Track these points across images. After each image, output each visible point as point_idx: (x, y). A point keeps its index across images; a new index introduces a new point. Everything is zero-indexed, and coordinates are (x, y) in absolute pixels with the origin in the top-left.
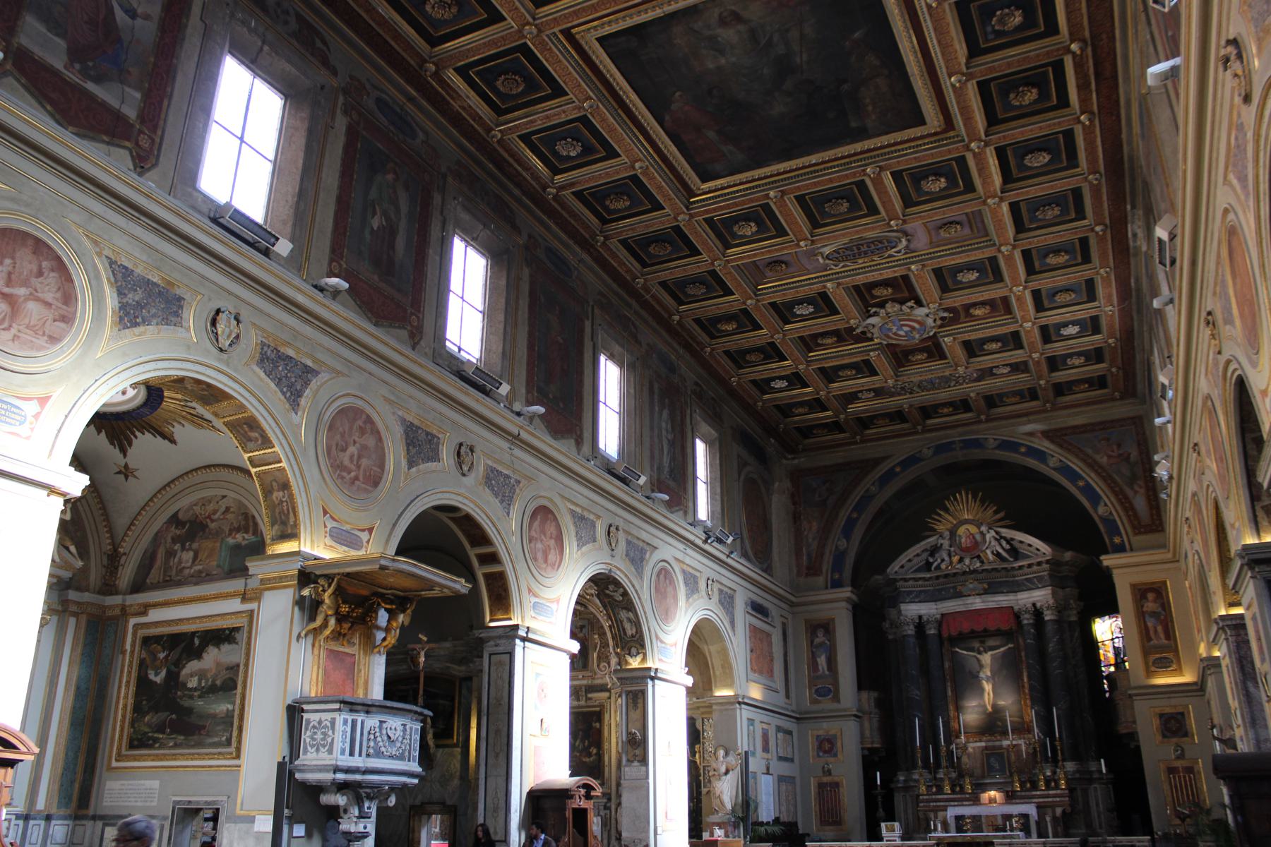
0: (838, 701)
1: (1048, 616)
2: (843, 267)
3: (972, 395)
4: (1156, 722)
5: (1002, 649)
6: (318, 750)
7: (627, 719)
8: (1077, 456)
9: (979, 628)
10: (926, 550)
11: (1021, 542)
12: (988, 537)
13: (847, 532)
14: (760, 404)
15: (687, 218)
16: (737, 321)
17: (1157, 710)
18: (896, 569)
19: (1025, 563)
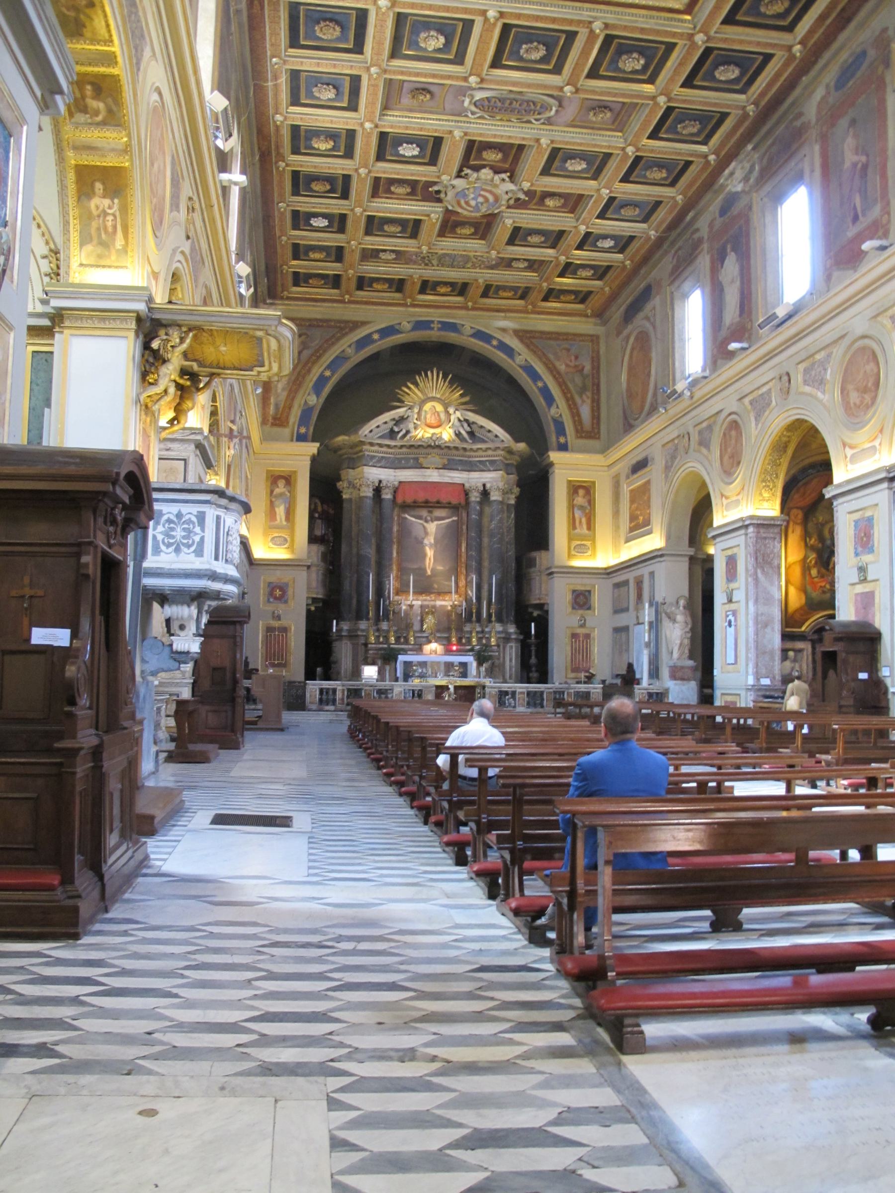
1: (495, 496)
2: (479, 118)
3: (481, 281)
4: (569, 597)
5: (447, 521)
6: (177, 550)
10: (394, 419)
11: (482, 427)
12: (452, 417)
16: (335, 142)
17: (572, 587)
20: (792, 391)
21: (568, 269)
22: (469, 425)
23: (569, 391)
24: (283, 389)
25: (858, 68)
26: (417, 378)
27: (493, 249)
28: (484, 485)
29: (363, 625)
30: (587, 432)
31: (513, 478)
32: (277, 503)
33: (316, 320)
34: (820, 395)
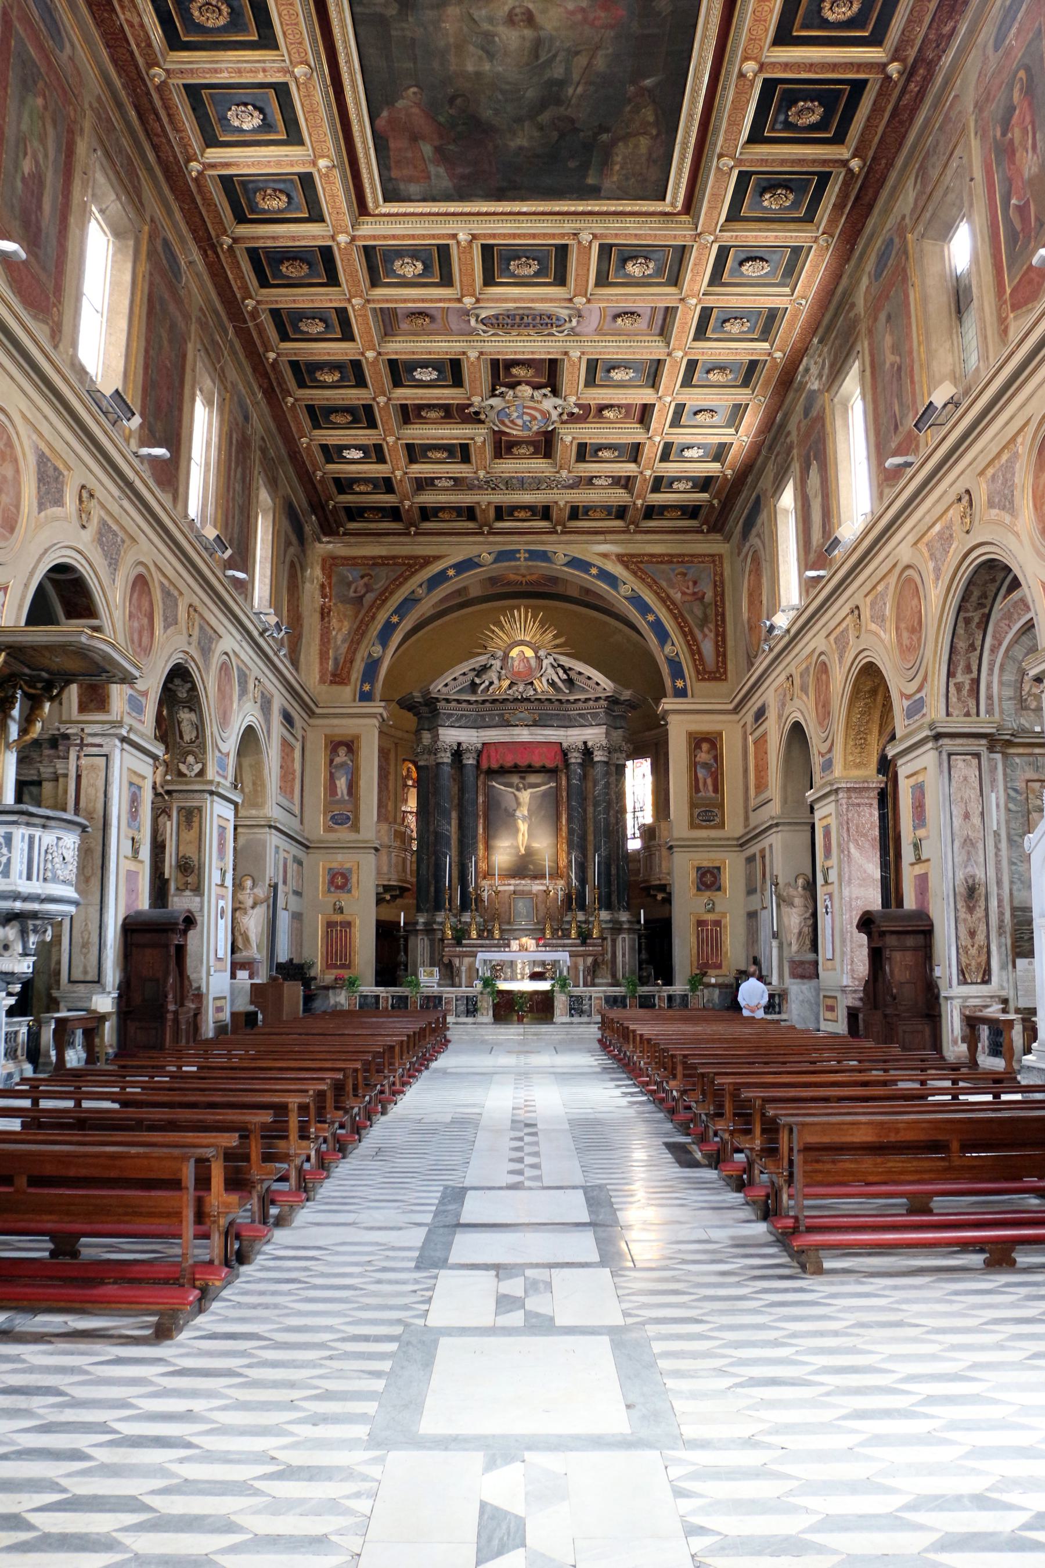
0: (358, 831)
1: (599, 756)
3: (562, 504)
4: (693, 875)
7: (178, 840)
8: (650, 587)
9: (523, 763)
11: (580, 673)
12: (545, 662)
13: (384, 637)
14: (319, 473)
15: (348, 239)
17: (696, 863)
19: (582, 697)
20: (863, 629)
21: (659, 484)
22: (565, 672)
24: (344, 641)
25: (888, 258)
27: (561, 468)
28: (585, 743)
29: (440, 917)
30: (710, 673)
32: (337, 775)
33: (381, 557)
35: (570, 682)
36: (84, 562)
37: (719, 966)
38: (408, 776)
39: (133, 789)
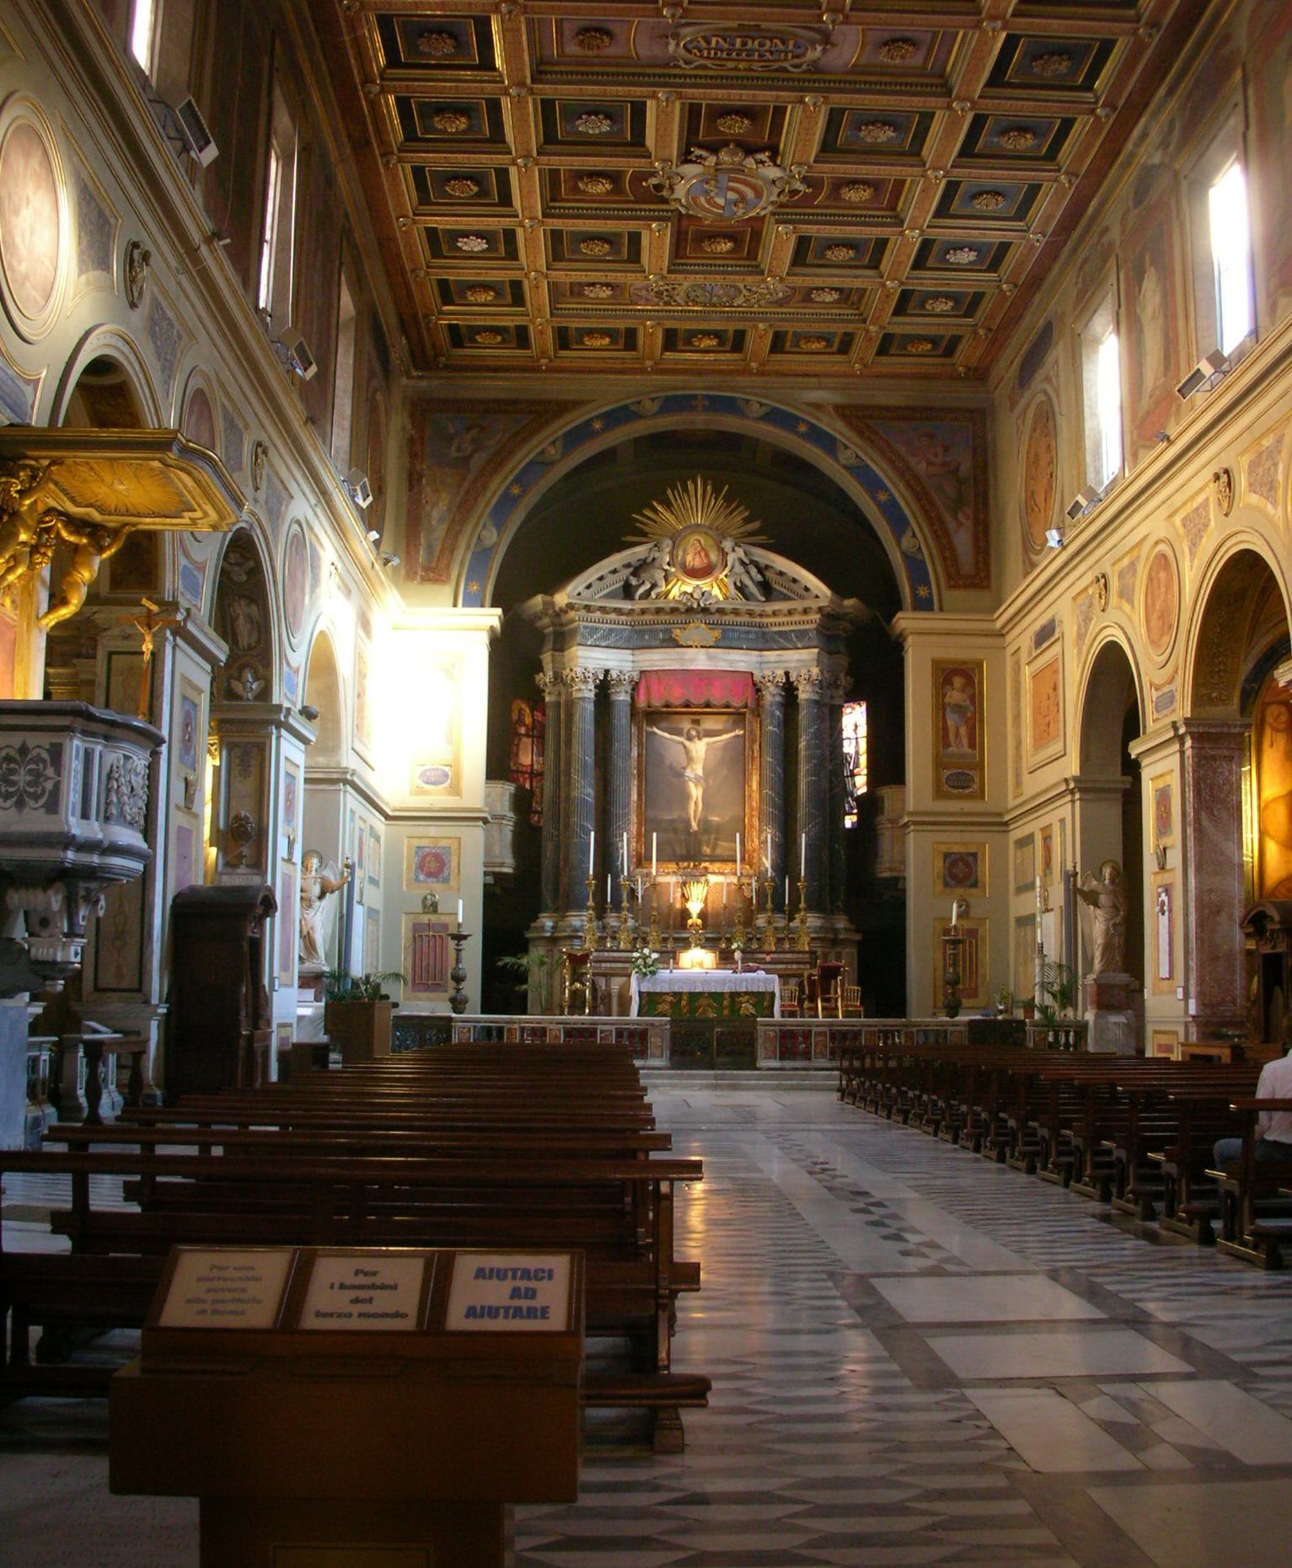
1: (804, 694)
4: (939, 864)
5: (725, 737)
6: (20, 804)
7: (228, 793)
8: (882, 452)
10: (628, 565)
11: (781, 574)
12: (731, 558)
16: (469, 118)
17: (944, 848)
18: (581, 588)
22: (760, 571)
23: (933, 505)
24: (441, 520)
26: (669, 492)
28: (787, 674)
31: (843, 660)
34: (1269, 507)
35: (766, 588)
36: (132, 357)
37: (976, 996)
38: (520, 721)
39: (187, 707)
